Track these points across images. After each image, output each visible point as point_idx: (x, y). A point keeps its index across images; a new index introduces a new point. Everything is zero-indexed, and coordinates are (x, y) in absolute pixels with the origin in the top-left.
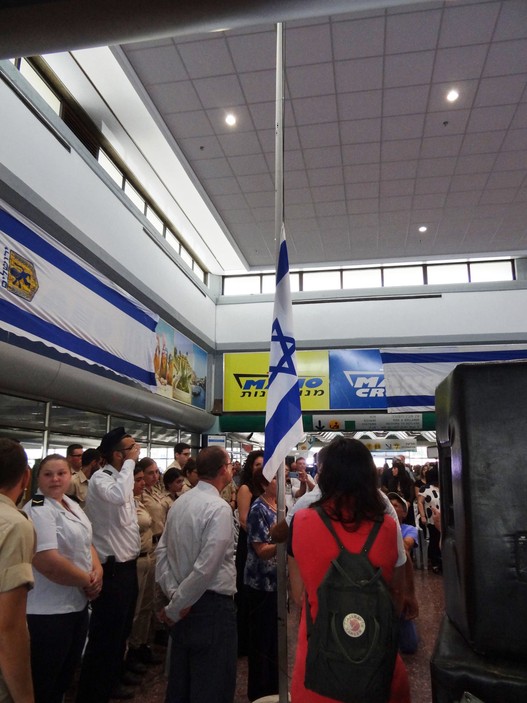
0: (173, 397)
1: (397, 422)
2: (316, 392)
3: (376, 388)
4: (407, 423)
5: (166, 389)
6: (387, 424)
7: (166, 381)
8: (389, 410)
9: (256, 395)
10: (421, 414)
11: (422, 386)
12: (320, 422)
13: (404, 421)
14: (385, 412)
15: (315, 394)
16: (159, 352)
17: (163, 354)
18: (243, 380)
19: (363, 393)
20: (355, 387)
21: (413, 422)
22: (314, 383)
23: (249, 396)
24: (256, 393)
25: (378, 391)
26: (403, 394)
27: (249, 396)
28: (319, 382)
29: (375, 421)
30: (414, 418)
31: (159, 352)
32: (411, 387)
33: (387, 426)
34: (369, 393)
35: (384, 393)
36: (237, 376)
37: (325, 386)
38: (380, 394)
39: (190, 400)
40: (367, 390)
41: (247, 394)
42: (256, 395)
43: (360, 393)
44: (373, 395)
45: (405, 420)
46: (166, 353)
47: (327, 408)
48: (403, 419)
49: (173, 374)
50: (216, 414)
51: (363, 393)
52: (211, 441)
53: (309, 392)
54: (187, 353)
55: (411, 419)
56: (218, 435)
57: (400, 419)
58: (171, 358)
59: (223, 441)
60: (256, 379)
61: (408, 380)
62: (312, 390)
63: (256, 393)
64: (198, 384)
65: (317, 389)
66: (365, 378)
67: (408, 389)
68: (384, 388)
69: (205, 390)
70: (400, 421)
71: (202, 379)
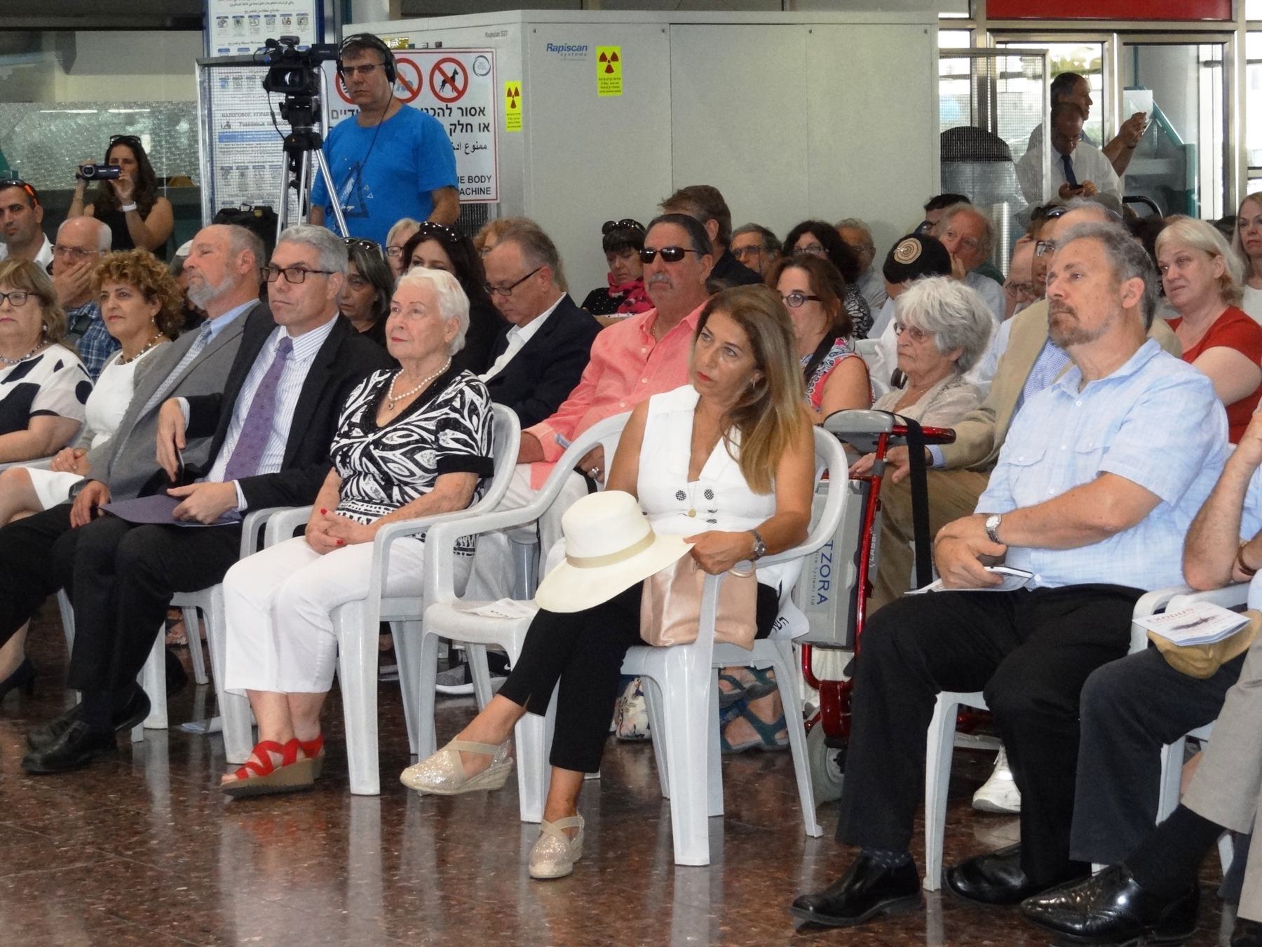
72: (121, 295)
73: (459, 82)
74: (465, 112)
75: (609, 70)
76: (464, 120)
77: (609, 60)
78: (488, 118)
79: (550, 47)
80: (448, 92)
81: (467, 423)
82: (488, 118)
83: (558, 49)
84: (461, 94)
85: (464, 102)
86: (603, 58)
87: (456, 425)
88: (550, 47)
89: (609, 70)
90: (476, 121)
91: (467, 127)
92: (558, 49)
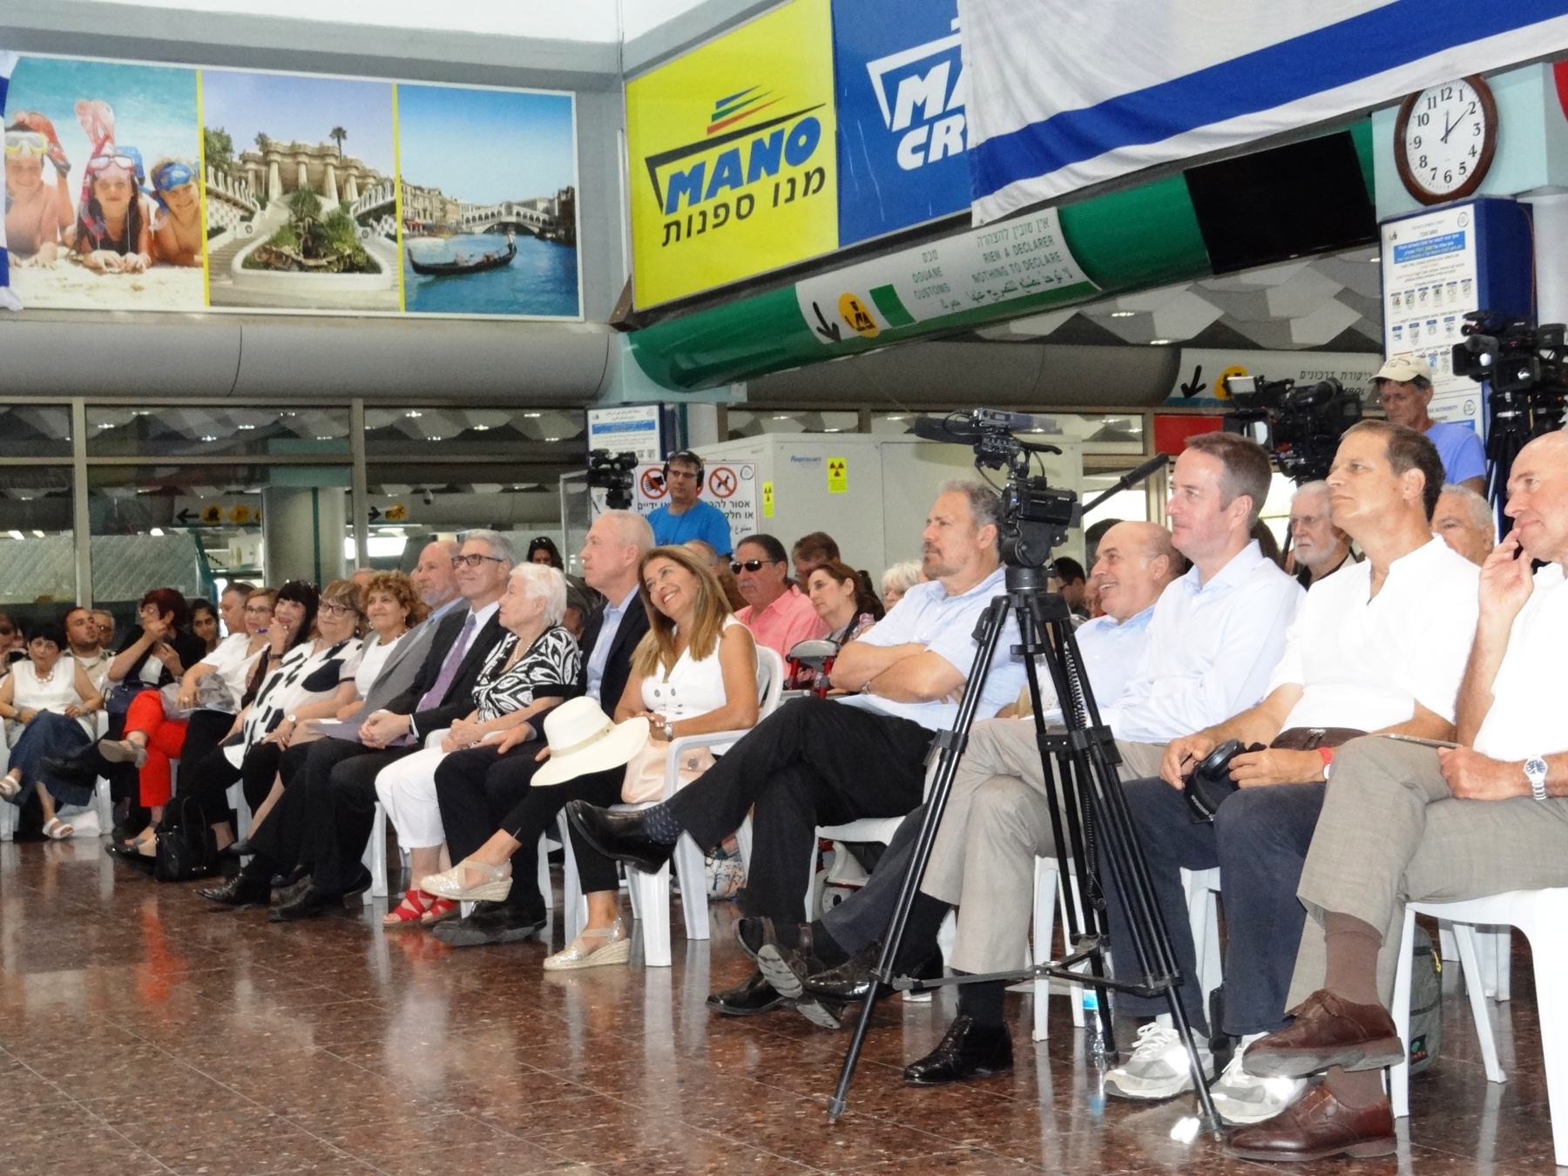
0: (212, 303)
1: (998, 264)
2: (808, 177)
3: (946, 114)
4: (1029, 265)
5: (140, 284)
6: (976, 279)
7: (142, 258)
8: (984, 208)
9: (689, 234)
10: (1051, 213)
11: (1060, 67)
12: (815, 305)
13: (1013, 259)
14: (963, 223)
15: (806, 193)
16: (63, 170)
17: (91, 172)
18: (665, 173)
19: (915, 150)
20: (895, 128)
21: (1042, 252)
22: (802, 140)
23: (678, 238)
24: (690, 219)
25: (948, 129)
26: (1010, 126)
27: (678, 238)
28: (811, 128)
29: (937, 272)
30: (1036, 235)
31: (63, 170)
32: (1026, 82)
33: (998, 284)
34: (925, 147)
35: (964, 134)
36: (654, 162)
37: (825, 154)
38: (956, 148)
39: (398, 297)
40: (919, 136)
41: (674, 229)
42: (689, 234)
43: (908, 160)
44: (936, 155)
45: (1019, 249)
46: (126, 162)
47: (829, 243)
48: (1011, 242)
49: (208, 223)
50: (620, 327)
51: (915, 150)
52: (598, 430)
53: (792, 181)
54: (339, 133)
55: (1029, 238)
56: (626, 404)
57: (999, 248)
58: (177, 174)
59: (650, 426)
60: (685, 165)
61: (1022, 48)
62: (798, 172)
63: (690, 219)
64: (479, 229)
65: (810, 164)
66: (916, 78)
67: (1019, 93)
68: (960, 110)
69: (568, 242)
70: (1003, 262)
71: (531, 204)
72: (384, 600)
73: (731, 483)
74: (735, 504)
75: (837, 474)
76: (735, 510)
77: (837, 468)
78: (752, 509)
79: (793, 459)
80: (722, 491)
81: (551, 661)
82: (752, 509)
83: (800, 460)
84: (732, 492)
85: (735, 498)
86: (832, 466)
87: (543, 664)
88: (793, 459)
89: (837, 474)
90: (743, 511)
91: (737, 515)
92: (800, 460)
